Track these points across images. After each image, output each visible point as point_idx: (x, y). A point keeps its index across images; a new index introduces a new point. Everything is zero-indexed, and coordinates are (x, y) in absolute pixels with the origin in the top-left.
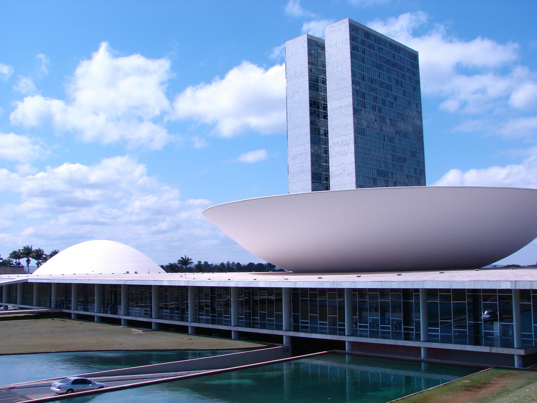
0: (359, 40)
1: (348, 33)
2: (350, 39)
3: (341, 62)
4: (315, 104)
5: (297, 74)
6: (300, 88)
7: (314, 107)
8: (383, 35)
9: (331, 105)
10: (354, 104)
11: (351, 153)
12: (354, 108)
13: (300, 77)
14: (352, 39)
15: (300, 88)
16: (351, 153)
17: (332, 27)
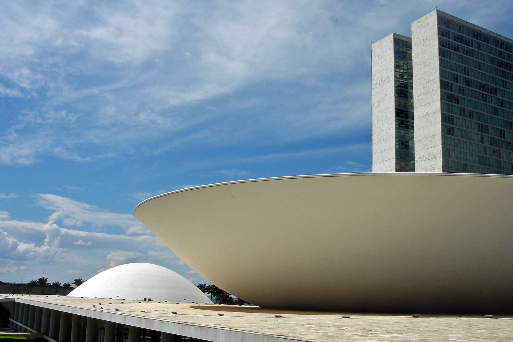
0: (451, 36)
1: (436, 26)
2: (439, 34)
3: (428, 62)
4: (403, 114)
5: (383, 79)
6: (386, 95)
7: (402, 117)
8: (485, 29)
9: (418, 112)
10: (442, 109)
11: (438, 168)
12: (443, 115)
13: (386, 83)
14: (442, 33)
15: (386, 95)
16: (438, 168)
17: (419, 22)
